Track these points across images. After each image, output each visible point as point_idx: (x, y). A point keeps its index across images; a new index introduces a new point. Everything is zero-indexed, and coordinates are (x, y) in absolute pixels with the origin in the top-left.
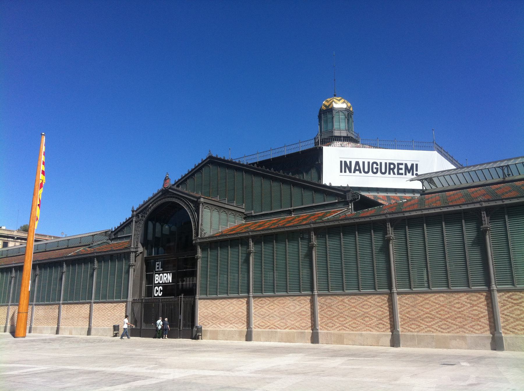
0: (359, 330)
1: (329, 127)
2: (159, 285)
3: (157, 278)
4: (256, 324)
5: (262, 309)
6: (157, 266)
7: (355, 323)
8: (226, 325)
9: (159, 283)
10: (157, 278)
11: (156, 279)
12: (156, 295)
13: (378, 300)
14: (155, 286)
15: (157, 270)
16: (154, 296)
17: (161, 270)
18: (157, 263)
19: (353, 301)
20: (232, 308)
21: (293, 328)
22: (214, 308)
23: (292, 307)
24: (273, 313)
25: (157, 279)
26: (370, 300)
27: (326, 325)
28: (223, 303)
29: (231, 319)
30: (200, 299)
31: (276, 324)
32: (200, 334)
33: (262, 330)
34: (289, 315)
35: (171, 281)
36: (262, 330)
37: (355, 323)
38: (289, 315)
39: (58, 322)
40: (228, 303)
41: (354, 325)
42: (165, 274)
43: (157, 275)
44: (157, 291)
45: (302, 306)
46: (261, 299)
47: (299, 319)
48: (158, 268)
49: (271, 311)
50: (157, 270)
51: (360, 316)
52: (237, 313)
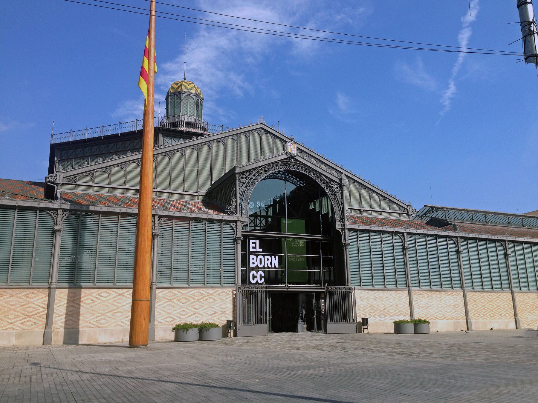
2: (257, 269)
3: (255, 261)
6: (252, 245)
8: (386, 317)
11: (252, 261)
12: (255, 281)
13: (504, 297)
15: (252, 250)
16: (250, 283)
17: (261, 250)
18: (251, 241)
22: (372, 300)
24: (431, 306)
25: (253, 261)
28: (381, 295)
29: (391, 311)
30: (157, 288)
31: (435, 315)
32: (366, 327)
34: (445, 308)
35: (277, 266)
38: (445, 308)
39: (47, 318)
40: (387, 295)
42: (266, 257)
43: (251, 257)
44: (254, 277)
45: (455, 300)
46: (420, 292)
47: (454, 311)
48: (255, 248)
50: (252, 250)
52: (397, 306)
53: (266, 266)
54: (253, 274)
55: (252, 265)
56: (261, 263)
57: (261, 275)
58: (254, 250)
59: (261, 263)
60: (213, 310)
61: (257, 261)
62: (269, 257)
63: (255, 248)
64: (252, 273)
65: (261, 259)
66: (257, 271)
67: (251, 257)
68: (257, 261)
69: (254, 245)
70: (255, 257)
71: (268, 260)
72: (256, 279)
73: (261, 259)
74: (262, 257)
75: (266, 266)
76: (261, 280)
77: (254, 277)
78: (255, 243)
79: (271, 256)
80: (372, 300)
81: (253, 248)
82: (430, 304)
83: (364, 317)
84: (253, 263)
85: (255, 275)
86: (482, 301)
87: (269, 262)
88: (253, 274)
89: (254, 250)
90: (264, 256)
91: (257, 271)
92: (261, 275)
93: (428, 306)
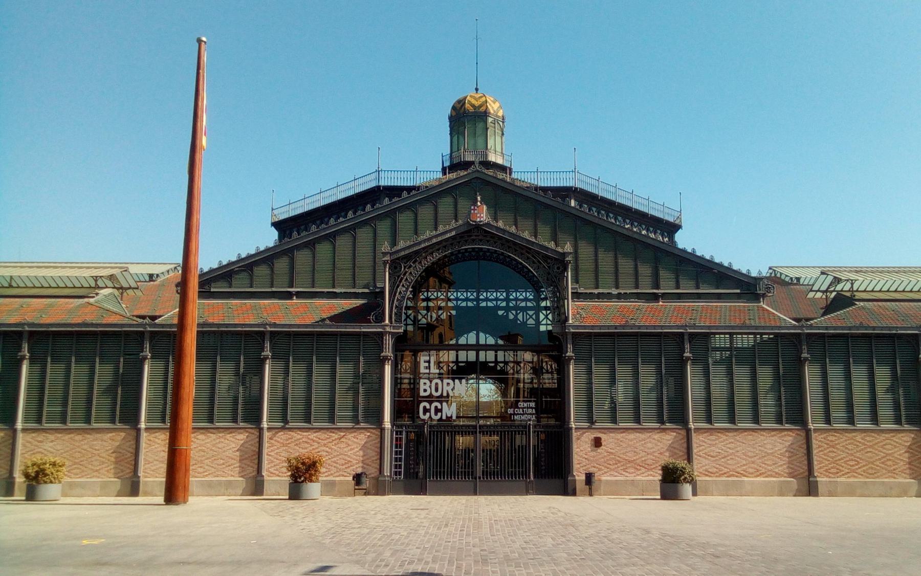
0: (878, 477)
1: (480, 141)
4: (701, 470)
5: (713, 448)
7: (872, 468)
8: (639, 472)
9: (431, 396)
10: (425, 387)
11: (422, 387)
14: (421, 402)
16: (419, 417)
19: (868, 438)
20: (649, 445)
21: (771, 476)
23: (769, 446)
26: (894, 439)
27: (826, 471)
29: (650, 462)
33: (714, 479)
36: (714, 479)
37: (872, 468)
41: (870, 471)
42: (446, 381)
44: (426, 410)
49: (731, 451)
51: (879, 459)
53: (445, 394)
54: (425, 407)
55: (422, 394)
56: (437, 390)
57: (436, 407)
58: (427, 371)
59: (437, 390)
60: (346, 458)
61: (430, 387)
62: (450, 381)
63: (429, 368)
64: (422, 405)
65: (437, 384)
66: (430, 403)
67: (422, 381)
68: (430, 387)
69: (427, 364)
70: (427, 381)
71: (448, 384)
72: (428, 414)
73: (437, 384)
74: (439, 381)
75: (445, 394)
76: (436, 414)
77: (426, 410)
78: (429, 362)
79: (453, 379)
80: (611, 446)
81: (426, 368)
82: (731, 451)
83: (592, 470)
84: (425, 391)
85: (428, 407)
86: (850, 447)
87: (449, 388)
88: (425, 407)
89: (427, 371)
90: (441, 379)
91: (430, 403)
92: (436, 407)
93: (726, 454)
